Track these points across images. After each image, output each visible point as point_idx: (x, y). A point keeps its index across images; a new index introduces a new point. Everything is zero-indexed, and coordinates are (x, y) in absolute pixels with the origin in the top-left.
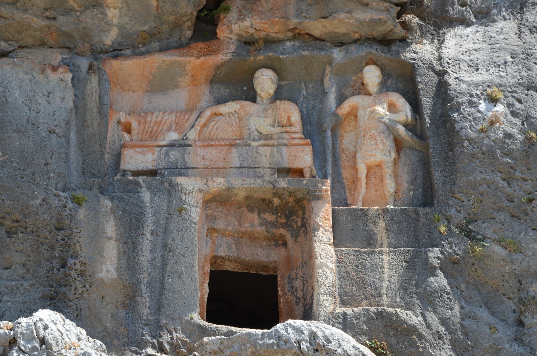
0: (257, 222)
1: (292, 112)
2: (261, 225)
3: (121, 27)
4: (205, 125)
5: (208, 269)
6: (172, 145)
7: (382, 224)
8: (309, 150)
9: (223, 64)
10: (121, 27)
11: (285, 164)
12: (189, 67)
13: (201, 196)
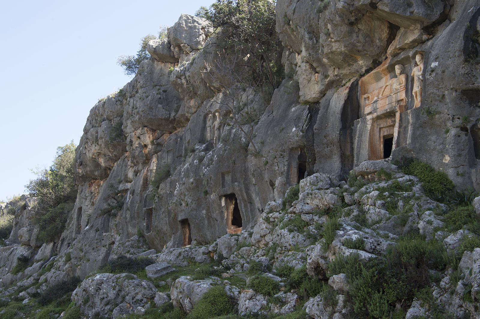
0: (391, 122)
1: (403, 78)
2: (392, 122)
3: (365, 65)
4: (384, 91)
5: (382, 140)
6: (374, 102)
7: (410, 115)
8: (404, 91)
9: (388, 68)
10: (365, 65)
11: (399, 99)
12: (381, 72)
13: (371, 120)
